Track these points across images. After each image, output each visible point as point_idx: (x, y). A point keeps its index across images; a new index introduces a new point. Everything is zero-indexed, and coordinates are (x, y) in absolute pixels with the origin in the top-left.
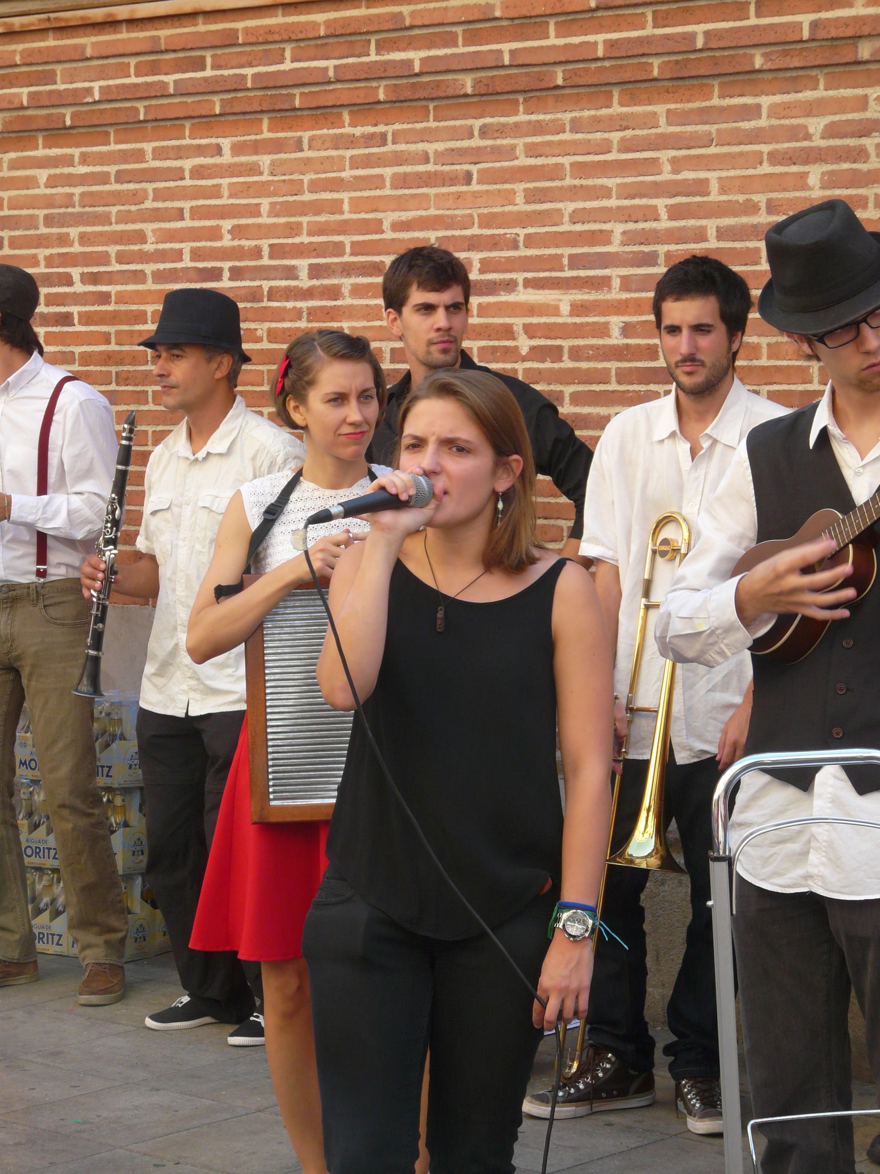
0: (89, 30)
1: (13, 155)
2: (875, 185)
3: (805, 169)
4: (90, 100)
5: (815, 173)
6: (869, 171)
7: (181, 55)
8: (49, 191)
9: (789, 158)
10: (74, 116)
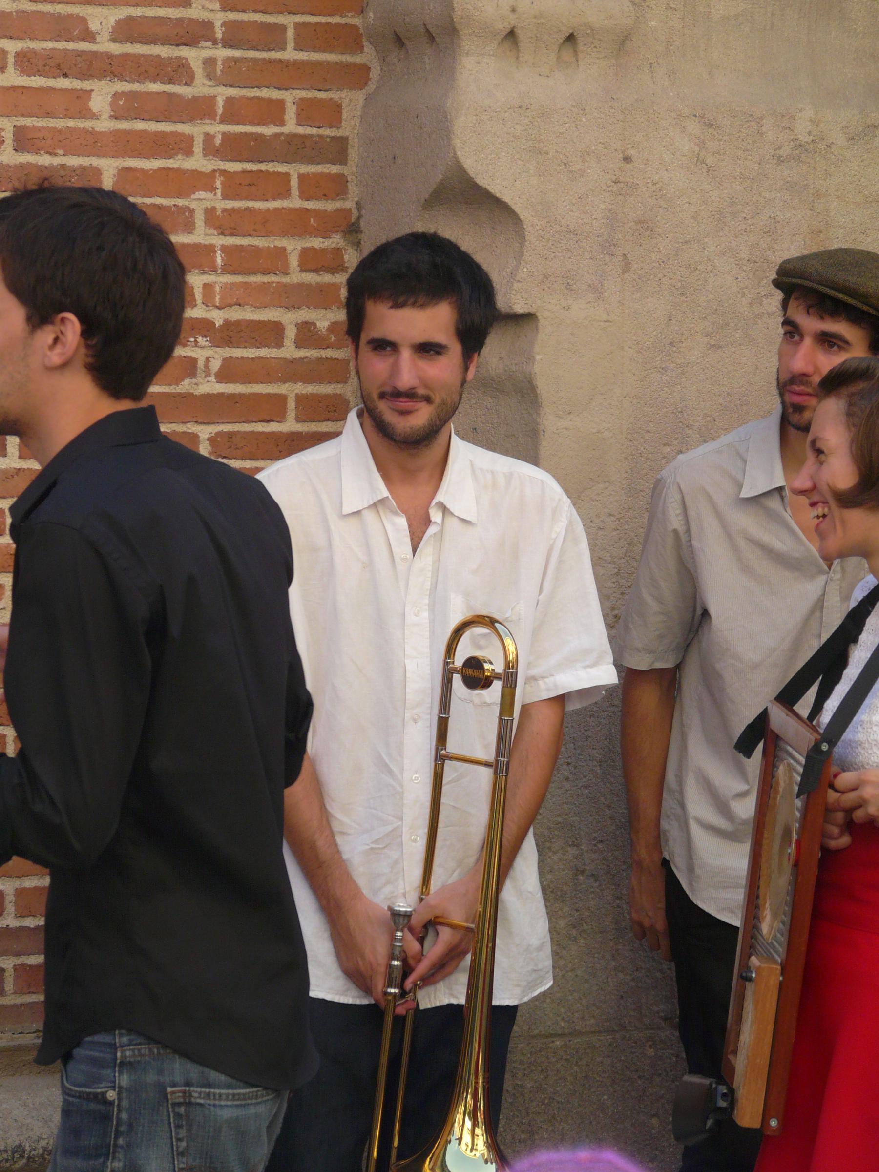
2: (207, 121)
3: (86, 85)
5: (102, 94)
6: (195, 99)
9: (59, 66)
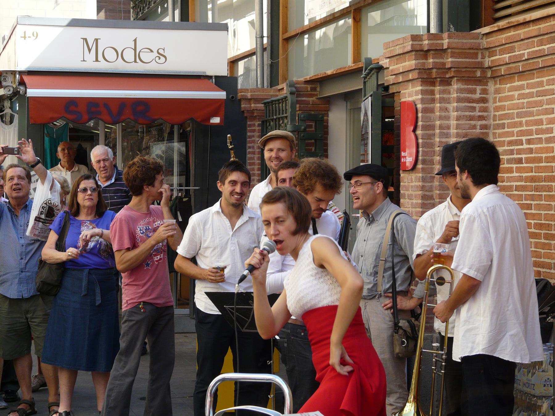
0: (522, 27)
1: (509, 85)
4: (524, 59)
7: (549, 36)
8: (518, 101)
10: (523, 66)
